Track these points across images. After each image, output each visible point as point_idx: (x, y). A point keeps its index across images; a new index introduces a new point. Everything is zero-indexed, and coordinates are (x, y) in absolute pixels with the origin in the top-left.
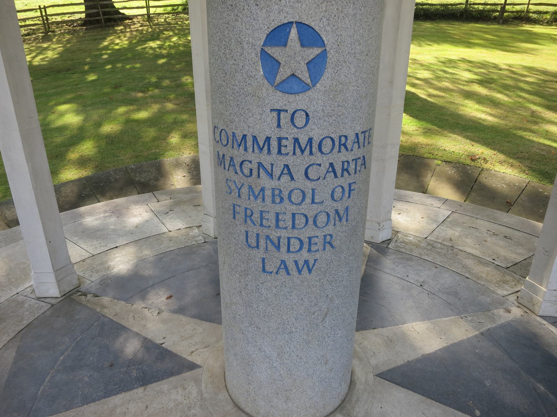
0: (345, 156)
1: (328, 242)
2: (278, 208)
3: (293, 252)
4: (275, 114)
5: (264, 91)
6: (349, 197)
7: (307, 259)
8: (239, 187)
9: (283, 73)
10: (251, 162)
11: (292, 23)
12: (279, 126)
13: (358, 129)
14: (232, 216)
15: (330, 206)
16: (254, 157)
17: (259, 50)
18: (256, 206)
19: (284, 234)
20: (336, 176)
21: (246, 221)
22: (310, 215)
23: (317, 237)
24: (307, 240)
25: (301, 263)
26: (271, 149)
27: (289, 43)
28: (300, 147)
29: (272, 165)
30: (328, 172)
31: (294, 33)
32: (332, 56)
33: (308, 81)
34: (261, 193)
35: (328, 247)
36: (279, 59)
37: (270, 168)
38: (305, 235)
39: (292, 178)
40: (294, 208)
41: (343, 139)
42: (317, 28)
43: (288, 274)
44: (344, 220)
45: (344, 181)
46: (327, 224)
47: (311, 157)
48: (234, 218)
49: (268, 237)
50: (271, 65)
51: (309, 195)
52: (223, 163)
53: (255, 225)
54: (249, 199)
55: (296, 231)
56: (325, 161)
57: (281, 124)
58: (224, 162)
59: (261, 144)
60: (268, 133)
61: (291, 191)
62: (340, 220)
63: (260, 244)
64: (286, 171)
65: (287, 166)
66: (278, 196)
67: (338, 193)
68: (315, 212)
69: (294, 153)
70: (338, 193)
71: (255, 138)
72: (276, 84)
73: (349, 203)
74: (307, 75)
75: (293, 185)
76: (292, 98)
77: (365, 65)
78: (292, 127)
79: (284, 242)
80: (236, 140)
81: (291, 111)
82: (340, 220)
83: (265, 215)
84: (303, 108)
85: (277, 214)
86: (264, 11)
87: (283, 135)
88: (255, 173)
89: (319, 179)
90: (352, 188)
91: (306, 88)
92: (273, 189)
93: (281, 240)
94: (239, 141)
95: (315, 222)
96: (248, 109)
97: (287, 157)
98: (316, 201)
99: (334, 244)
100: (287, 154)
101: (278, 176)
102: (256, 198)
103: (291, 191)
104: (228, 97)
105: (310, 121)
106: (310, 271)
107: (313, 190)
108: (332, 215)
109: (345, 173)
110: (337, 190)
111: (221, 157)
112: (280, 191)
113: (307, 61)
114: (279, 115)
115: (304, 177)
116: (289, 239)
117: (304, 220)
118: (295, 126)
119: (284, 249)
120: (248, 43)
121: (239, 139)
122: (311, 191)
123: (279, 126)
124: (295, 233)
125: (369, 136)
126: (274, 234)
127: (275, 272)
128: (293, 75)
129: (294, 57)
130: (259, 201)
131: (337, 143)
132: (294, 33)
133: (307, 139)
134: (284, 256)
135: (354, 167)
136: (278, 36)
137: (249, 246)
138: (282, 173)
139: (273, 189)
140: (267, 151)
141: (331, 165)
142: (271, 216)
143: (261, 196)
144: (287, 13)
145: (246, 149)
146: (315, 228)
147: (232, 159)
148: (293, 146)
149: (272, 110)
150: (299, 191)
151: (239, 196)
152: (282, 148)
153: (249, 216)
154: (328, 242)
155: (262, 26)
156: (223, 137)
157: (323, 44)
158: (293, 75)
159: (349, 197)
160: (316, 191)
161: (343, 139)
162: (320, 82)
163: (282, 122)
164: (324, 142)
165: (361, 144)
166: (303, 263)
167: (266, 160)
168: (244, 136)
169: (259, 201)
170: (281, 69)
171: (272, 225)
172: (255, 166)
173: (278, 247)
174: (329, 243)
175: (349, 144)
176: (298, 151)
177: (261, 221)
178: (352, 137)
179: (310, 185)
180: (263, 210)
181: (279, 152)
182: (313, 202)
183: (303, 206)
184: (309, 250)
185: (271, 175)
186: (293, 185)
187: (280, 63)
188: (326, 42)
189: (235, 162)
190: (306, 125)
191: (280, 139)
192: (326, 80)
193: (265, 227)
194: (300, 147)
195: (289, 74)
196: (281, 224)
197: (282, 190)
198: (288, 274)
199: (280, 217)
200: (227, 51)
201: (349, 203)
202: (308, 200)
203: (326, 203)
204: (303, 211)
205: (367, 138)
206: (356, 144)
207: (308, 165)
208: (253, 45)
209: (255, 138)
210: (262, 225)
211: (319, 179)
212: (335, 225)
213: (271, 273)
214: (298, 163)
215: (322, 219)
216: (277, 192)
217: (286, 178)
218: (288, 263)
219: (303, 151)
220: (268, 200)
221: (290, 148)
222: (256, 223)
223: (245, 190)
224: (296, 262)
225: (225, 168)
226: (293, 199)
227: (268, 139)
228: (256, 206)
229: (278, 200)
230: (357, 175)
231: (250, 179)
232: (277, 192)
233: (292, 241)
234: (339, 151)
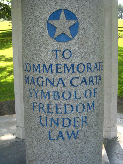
0: (90, 74)
1: (84, 121)
2: (57, 102)
3: (66, 127)
4: (54, 52)
5: (49, 41)
6: (94, 96)
7: (73, 130)
8: (36, 92)
10: (42, 78)
11: (61, 10)
12: (56, 58)
13: (96, 61)
14: (33, 109)
15: (84, 100)
16: (44, 75)
17: (46, 22)
18: (45, 101)
19: (60, 116)
20: (86, 84)
21: (40, 111)
22: (74, 105)
23: (78, 118)
24: (73, 119)
25: (70, 133)
26: (53, 70)
27: (61, 18)
28: (67, 68)
29: (53, 78)
30: (82, 82)
31: (63, 14)
32: (81, 25)
33: (70, 36)
34: (48, 94)
35: (84, 124)
36: (56, 26)
37: (52, 80)
38: (72, 117)
39: (64, 85)
40: (65, 102)
41: (89, 65)
42: (73, 12)
43: (63, 139)
44: (92, 108)
45: (91, 87)
46: (83, 110)
47: (73, 74)
48: (34, 110)
49: (52, 119)
50: (52, 29)
51: (73, 94)
52: (28, 81)
53: (45, 112)
54: (42, 98)
55: (67, 114)
56: (81, 76)
57: (58, 57)
58: (29, 80)
59: (48, 68)
60: (51, 62)
61: (63, 93)
62: (90, 108)
63: (48, 123)
64: (60, 82)
65: (61, 79)
66: (57, 95)
67: (88, 93)
68: (77, 104)
69: (65, 72)
70: (88, 93)
71: (44, 65)
72: (54, 38)
73: (94, 99)
74: (70, 33)
75: (64, 89)
76: (62, 44)
77: (97, 30)
78: (63, 58)
79: (60, 121)
80: (35, 68)
81: (62, 51)
82: (90, 108)
83: (50, 107)
84: (68, 49)
85: (57, 106)
86: (49, 5)
87: (59, 62)
88: (45, 84)
89: (78, 85)
90: (95, 92)
91: (70, 39)
92: (54, 92)
93: (59, 120)
94: (36, 68)
95: (77, 109)
96: (41, 51)
97: (61, 74)
98: (77, 97)
99: (88, 122)
100: (61, 72)
101: (56, 84)
102: (45, 97)
103: (63, 93)
104: (31, 46)
105: (72, 55)
106: (75, 137)
107: (75, 91)
108: (86, 105)
109: (91, 83)
110: (87, 92)
111: (27, 78)
112: (58, 92)
113: (69, 26)
114: (56, 53)
115: (70, 84)
116: (63, 119)
117: (71, 108)
118: (65, 58)
119: (60, 125)
120: (41, 19)
121: (36, 66)
122: (74, 92)
123: (56, 58)
124: (67, 116)
125: (102, 66)
126: (55, 117)
127: (56, 139)
128: (63, 33)
129: (63, 25)
130: (47, 98)
131: (86, 67)
132: (63, 14)
133: (71, 64)
134: (60, 129)
135: (95, 80)
136: (55, 15)
137: (42, 125)
138: (59, 82)
139: (54, 92)
140: (50, 71)
141: (84, 78)
142: (54, 107)
143: (48, 96)
144: (59, 5)
145: (40, 72)
146: (77, 113)
147: (32, 78)
148: (64, 68)
149: (53, 50)
150: (68, 92)
151: (36, 97)
152: (58, 69)
153: (41, 108)
155: (48, 11)
156: (28, 67)
157: (76, 19)
158: (63, 33)
159: (94, 96)
160: (77, 92)
161: (89, 65)
162: (76, 36)
163: (58, 56)
164: (79, 66)
165: (98, 69)
166: (71, 133)
167: (50, 76)
168: (39, 65)
169: (47, 98)
170: (57, 30)
171: (54, 112)
172: (44, 80)
173: (58, 124)
174: (85, 121)
175: (92, 68)
176: (66, 70)
177: (48, 110)
178: (93, 65)
179: (73, 89)
180: (49, 103)
181: (57, 72)
182: (75, 98)
183: (70, 100)
184: (74, 125)
185: (53, 84)
186: (64, 89)
187: (56, 28)
188: (78, 18)
189: (34, 79)
190: (70, 58)
191: (57, 65)
192: (79, 35)
193: (50, 113)
194: (67, 68)
195: (61, 33)
196: (59, 111)
197: (59, 92)
198: (63, 139)
199: (58, 107)
200: (31, 25)
201: (94, 99)
202: (73, 97)
203: (82, 99)
204: (70, 103)
205: (101, 66)
206: (96, 68)
207: (72, 78)
208: (43, 20)
209: (44, 65)
210: (48, 112)
211: (78, 85)
212: (87, 111)
213: (54, 139)
214: (67, 77)
215: (80, 108)
216: (56, 93)
217: (61, 85)
218: (63, 133)
219: (69, 71)
220: (52, 97)
221: (63, 69)
222: (45, 111)
223: (39, 94)
224: (67, 132)
225: (29, 84)
226: (65, 97)
227: (51, 65)
228: (45, 101)
229: (57, 97)
230: (97, 85)
231: (42, 87)
232: (56, 93)
233: (65, 120)
234: (88, 71)
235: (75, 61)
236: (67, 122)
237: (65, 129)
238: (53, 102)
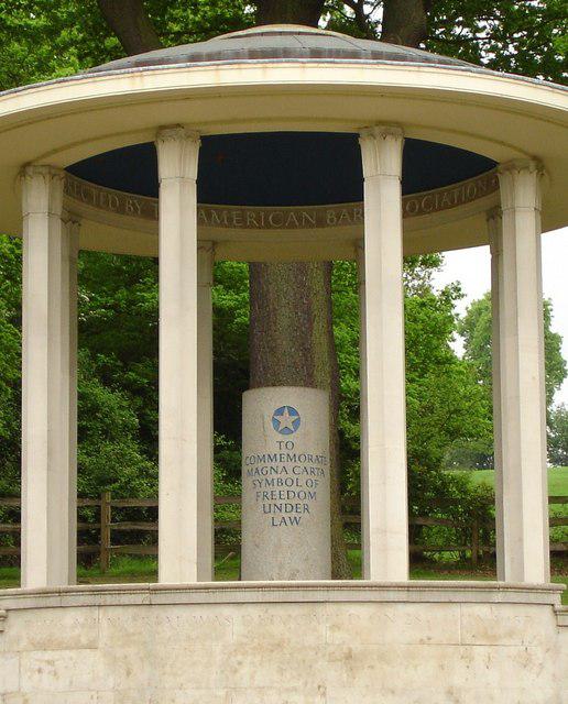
1: (306, 509)
15: (307, 489)
16: (269, 465)
18: (269, 489)
31: (286, 411)
50: (277, 423)
66: (280, 482)
119: (283, 510)
126: (278, 502)
129: (286, 420)
136: (280, 412)
142: (278, 492)
154: (306, 509)
167: (274, 464)
172: (269, 469)
178: (314, 457)
214: (290, 465)
215: (302, 495)
223: (264, 482)
228: (269, 489)
236: (289, 507)
237: (289, 515)
238: (277, 489)
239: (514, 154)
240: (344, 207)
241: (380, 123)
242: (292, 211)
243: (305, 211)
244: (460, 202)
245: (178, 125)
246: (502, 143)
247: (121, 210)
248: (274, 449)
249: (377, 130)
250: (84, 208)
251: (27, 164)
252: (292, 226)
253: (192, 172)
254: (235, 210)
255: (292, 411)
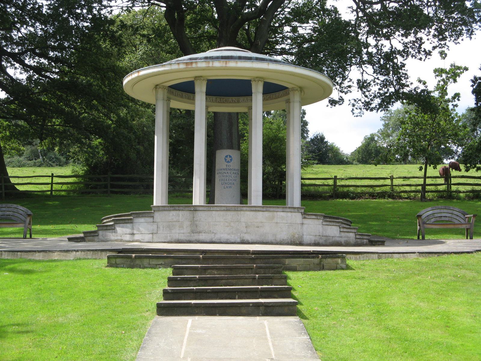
1: (233, 184)
9: (227, 161)
15: (234, 178)
16: (223, 171)
50: (226, 160)
66: (226, 176)
136: (227, 156)
154: (233, 184)
167: (225, 171)
214: (229, 172)
228: (223, 178)
235: (231, 168)
239: (294, 86)
240: (245, 98)
241: (257, 78)
242: (230, 99)
243: (234, 98)
244: (278, 98)
245: (201, 77)
246: (291, 83)
247: (182, 97)
248: (225, 167)
249: (256, 79)
250: (172, 96)
251: (157, 85)
252: (230, 102)
253: (204, 89)
254: (214, 98)
255: (230, 157)
